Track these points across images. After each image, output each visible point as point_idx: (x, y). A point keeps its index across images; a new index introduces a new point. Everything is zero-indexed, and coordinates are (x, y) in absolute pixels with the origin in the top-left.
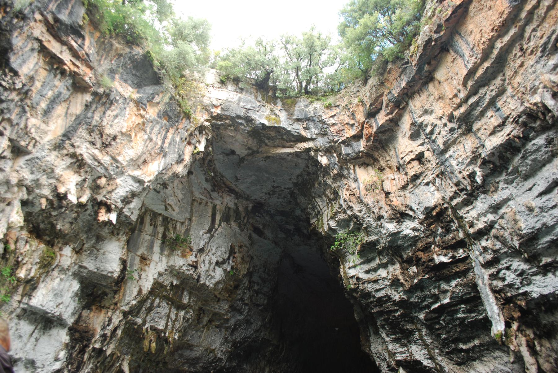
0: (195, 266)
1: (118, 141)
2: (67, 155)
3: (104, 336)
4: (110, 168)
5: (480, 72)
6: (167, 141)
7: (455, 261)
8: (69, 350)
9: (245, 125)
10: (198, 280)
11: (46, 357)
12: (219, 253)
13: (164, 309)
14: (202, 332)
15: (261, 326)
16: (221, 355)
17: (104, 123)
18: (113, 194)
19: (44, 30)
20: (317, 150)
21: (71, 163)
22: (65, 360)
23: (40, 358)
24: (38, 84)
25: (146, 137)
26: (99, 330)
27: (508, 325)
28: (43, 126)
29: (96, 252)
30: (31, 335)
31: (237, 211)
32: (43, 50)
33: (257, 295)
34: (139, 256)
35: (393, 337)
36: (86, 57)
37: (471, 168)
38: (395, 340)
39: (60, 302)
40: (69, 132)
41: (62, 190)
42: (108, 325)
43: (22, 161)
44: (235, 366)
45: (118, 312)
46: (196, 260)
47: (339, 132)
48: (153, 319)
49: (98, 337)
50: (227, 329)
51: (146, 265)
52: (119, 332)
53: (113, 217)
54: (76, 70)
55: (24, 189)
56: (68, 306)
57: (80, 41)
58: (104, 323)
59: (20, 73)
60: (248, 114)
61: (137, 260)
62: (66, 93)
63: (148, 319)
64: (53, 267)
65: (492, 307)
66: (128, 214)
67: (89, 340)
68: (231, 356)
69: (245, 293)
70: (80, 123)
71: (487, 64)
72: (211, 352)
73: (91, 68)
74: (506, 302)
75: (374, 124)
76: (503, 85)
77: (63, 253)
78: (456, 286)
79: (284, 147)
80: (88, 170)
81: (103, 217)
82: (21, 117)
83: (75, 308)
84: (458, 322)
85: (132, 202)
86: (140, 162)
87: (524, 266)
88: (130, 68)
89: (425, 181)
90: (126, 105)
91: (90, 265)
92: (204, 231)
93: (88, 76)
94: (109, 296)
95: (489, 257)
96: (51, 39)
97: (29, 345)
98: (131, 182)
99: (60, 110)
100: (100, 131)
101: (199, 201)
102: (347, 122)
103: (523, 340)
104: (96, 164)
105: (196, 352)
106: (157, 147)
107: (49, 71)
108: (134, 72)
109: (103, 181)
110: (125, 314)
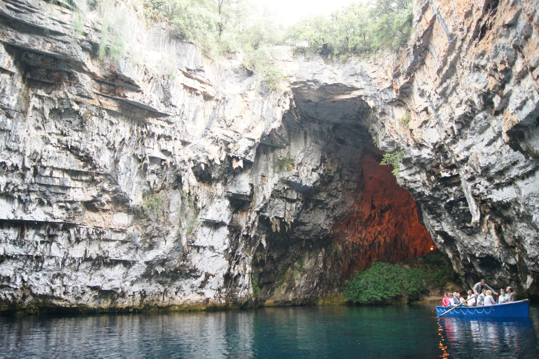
0: (297, 175)
3: (248, 228)
4: (234, 138)
5: (444, 72)
6: (264, 110)
7: (453, 177)
10: (301, 184)
12: (313, 163)
14: (311, 213)
15: (354, 204)
20: (366, 96)
24: (186, 106)
25: (251, 113)
26: (244, 224)
27: (482, 216)
30: (209, 234)
31: (322, 133)
32: (185, 87)
33: (348, 183)
35: (432, 216)
36: (208, 81)
37: (450, 123)
38: (433, 218)
41: (211, 158)
42: (249, 221)
43: (188, 147)
44: (338, 233)
47: (379, 84)
48: (276, 212)
49: (244, 228)
50: (328, 209)
52: (256, 224)
53: (241, 164)
54: (204, 90)
59: (177, 105)
61: (260, 178)
65: (473, 207)
67: (240, 231)
68: (334, 227)
71: (446, 68)
73: (212, 86)
74: (482, 202)
75: (398, 83)
76: (457, 81)
78: (456, 190)
79: (343, 94)
84: (461, 211)
87: (487, 184)
89: (431, 126)
91: (233, 190)
93: (210, 91)
95: (469, 176)
97: (209, 239)
102: (383, 77)
103: (493, 225)
104: (226, 137)
110: (258, 212)
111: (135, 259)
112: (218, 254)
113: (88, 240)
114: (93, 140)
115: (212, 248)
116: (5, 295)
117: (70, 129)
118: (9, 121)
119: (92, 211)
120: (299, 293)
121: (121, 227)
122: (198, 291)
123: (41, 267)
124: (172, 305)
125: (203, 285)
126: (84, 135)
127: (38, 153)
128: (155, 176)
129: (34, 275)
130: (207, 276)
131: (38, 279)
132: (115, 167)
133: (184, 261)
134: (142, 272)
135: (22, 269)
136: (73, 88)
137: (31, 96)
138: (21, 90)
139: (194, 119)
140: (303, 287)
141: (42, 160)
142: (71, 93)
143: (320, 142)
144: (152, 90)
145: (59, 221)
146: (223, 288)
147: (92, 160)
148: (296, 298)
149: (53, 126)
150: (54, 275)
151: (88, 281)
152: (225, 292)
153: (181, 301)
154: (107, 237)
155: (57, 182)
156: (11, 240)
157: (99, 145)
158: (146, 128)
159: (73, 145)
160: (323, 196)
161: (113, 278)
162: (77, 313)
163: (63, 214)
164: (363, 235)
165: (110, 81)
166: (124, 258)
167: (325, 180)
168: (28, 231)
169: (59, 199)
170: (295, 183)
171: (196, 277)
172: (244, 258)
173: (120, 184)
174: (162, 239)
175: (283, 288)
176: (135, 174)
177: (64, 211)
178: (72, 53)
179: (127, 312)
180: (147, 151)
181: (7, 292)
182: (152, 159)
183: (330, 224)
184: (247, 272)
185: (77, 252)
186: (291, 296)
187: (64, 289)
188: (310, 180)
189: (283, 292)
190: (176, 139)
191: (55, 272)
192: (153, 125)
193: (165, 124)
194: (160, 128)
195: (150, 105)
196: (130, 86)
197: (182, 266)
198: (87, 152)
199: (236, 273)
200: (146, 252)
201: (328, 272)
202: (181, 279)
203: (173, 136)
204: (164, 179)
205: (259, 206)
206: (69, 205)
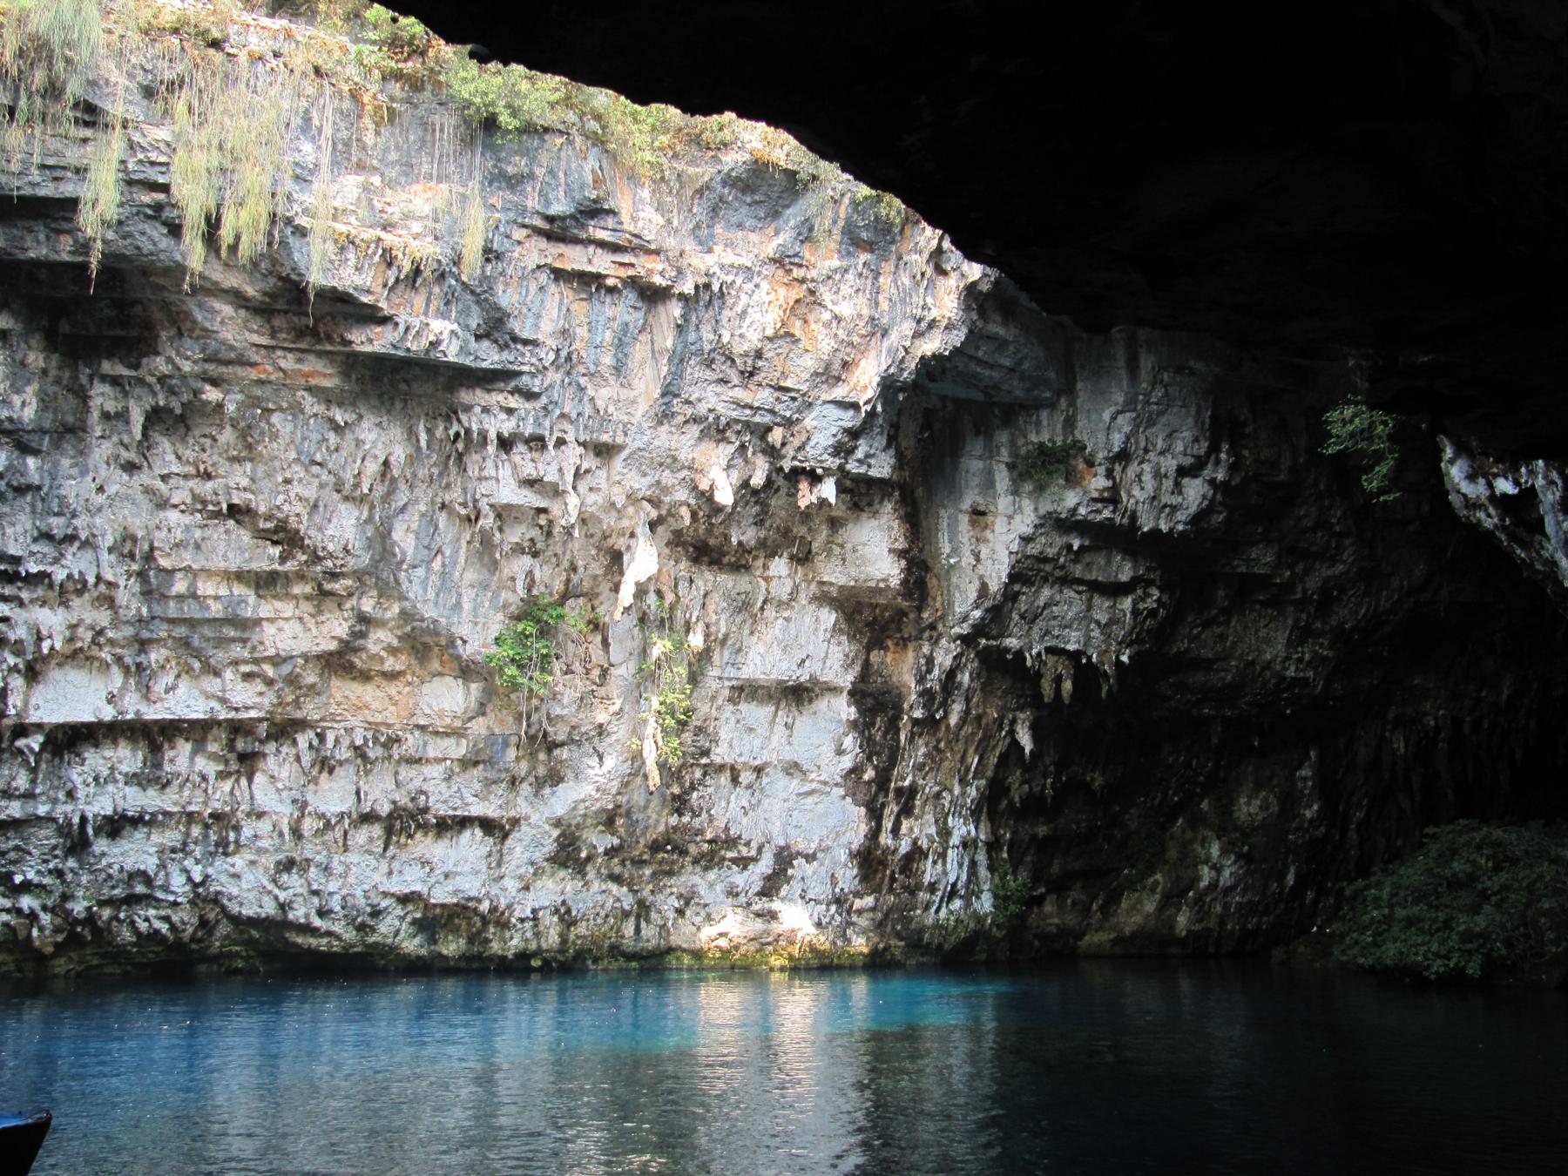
0: (1112, 498)
2: (686, 422)
3: (927, 695)
12: (1180, 447)
13: (1070, 603)
14: (1228, 623)
16: (1297, 670)
18: (808, 448)
19: (543, 243)
24: (582, 332)
28: (625, 394)
29: (837, 550)
30: (773, 721)
32: (559, 275)
34: (966, 512)
36: (636, 241)
41: (704, 485)
42: (929, 671)
43: (618, 462)
45: (943, 641)
46: (1109, 484)
48: (1047, 632)
49: (914, 697)
50: (1301, 604)
51: (986, 527)
53: (828, 490)
54: (631, 272)
57: (610, 222)
58: (919, 669)
59: (540, 337)
61: (964, 520)
64: (759, 605)
66: (862, 470)
70: (682, 361)
73: (657, 252)
77: (770, 573)
80: (739, 427)
81: (806, 497)
82: (581, 401)
83: (847, 656)
85: (856, 447)
91: (835, 575)
92: (1113, 409)
93: (656, 272)
96: (562, 248)
97: (775, 739)
99: (639, 351)
104: (748, 412)
107: (589, 299)
108: (749, 200)
110: (967, 640)
111: (512, 813)
112: (821, 787)
113: (359, 761)
114: (287, 481)
116: (147, 919)
117: (215, 458)
118: (31, 462)
119: (354, 679)
120: (1219, 909)
121: (448, 721)
122: (755, 907)
123: (237, 842)
124: (670, 950)
125: (770, 887)
126: (261, 469)
127: (134, 539)
128: (527, 560)
129: (220, 863)
131: (236, 876)
132: (384, 550)
133: (680, 815)
134: (545, 850)
135: (182, 850)
136: (188, 342)
137: (84, 380)
138: (45, 372)
139: (618, 369)
141: (157, 553)
142: (187, 358)
143: (1199, 366)
144: (432, 307)
145: (253, 714)
146: (858, 895)
147: (302, 539)
148: (1207, 930)
149: (167, 455)
150: (278, 863)
151: (385, 879)
152: (873, 909)
154: (412, 751)
155: (216, 610)
156: (126, 775)
157: (310, 493)
158: (459, 421)
159: (236, 501)
160: (1262, 558)
161: (456, 870)
162: (360, 968)
163: (261, 694)
164: (1506, 692)
165: (289, 302)
166: (477, 809)
167: (1244, 508)
168: (172, 748)
169: (234, 655)
171: (743, 863)
172: (938, 796)
173: (411, 595)
174: (587, 747)
175: (1153, 890)
176: (462, 560)
177: (261, 687)
178: (138, 248)
179: (518, 968)
180: (483, 488)
181: (152, 912)
182: (504, 514)
184: (955, 840)
185: (333, 796)
187: (316, 900)
188: (1174, 509)
189: (1150, 907)
190: (561, 442)
191: (281, 856)
192: (478, 410)
193: (514, 402)
194: (503, 416)
195: (432, 355)
196: (350, 309)
197: (676, 829)
198: (279, 515)
199: (905, 846)
200: (547, 791)
201: (1352, 835)
203: (547, 434)
204: (566, 564)
205: (965, 619)
206: (269, 670)
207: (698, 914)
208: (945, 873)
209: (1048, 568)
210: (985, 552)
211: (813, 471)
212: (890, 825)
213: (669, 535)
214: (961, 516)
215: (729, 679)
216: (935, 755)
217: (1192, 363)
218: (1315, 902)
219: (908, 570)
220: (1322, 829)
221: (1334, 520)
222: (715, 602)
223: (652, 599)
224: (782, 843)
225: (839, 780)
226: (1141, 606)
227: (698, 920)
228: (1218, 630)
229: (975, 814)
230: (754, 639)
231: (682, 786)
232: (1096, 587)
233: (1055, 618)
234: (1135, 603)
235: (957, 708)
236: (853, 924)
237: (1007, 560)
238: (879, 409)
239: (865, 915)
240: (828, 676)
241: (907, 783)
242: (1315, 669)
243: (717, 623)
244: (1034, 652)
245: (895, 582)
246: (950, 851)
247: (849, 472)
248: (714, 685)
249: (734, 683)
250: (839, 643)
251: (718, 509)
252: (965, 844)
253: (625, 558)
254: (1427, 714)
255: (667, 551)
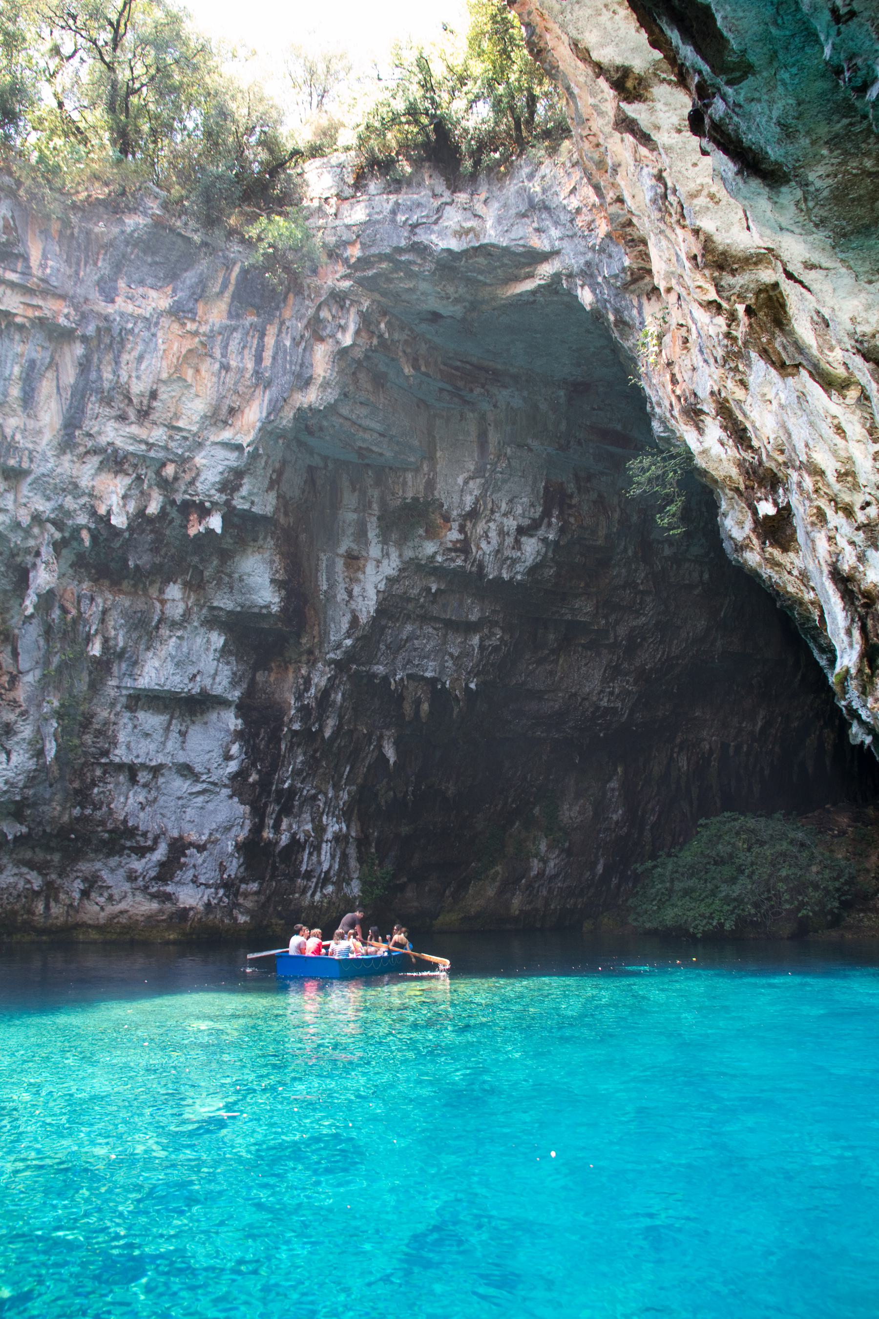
0: (463, 548)
1: (163, 396)
2: (87, 453)
3: (305, 711)
4: (172, 444)
6: (268, 355)
8: (247, 742)
9: (419, 261)
11: (207, 757)
12: (519, 510)
13: (428, 638)
16: (609, 701)
17: (124, 379)
18: (198, 484)
20: (570, 276)
21: (101, 462)
22: (243, 756)
23: (198, 760)
25: (217, 366)
28: (31, 424)
29: (226, 579)
30: (167, 729)
36: (42, 285)
39: (195, 672)
40: (73, 417)
41: (102, 510)
42: (307, 690)
43: (25, 488)
45: (320, 665)
46: (462, 537)
48: (409, 662)
49: (293, 712)
51: (359, 569)
53: (215, 522)
55: (49, 526)
56: (216, 674)
58: (298, 688)
60: (416, 239)
61: (340, 564)
62: (41, 356)
63: (399, 663)
66: (246, 506)
69: (636, 571)
72: (584, 699)
79: (517, 279)
83: (234, 674)
85: (241, 485)
86: (222, 415)
88: (137, 256)
90: (153, 330)
91: (225, 602)
92: (466, 475)
93: (61, 313)
94: (292, 641)
97: (170, 745)
98: (221, 453)
99: (46, 387)
100: (122, 393)
101: (444, 414)
105: (552, 703)
106: (248, 376)
108: (149, 260)
109: (170, 470)
110: (340, 666)
112: (212, 787)
115: (186, 771)
120: (545, 893)
125: (167, 870)
130: (179, 847)
133: (83, 808)
140: (556, 876)
143: (535, 444)
146: (243, 880)
152: (257, 893)
153: (102, 914)
164: (760, 724)
170: (459, 573)
171: (142, 852)
172: (314, 798)
175: (494, 879)
183: (629, 693)
184: (329, 835)
186: (517, 903)
188: (514, 561)
189: (491, 892)
197: (78, 819)
199: (285, 839)
201: (647, 834)
202: (92, 855)
205: (339, 646)
207: (101, 895)
208: (320, 863)
209: (410, 606)
210: (356, 590)
211: (202, 503)
212: (272, 822)
213: (72, 557)
214: (337, 559)
215: (127, 688)
216: (312, 764)
217: (530, 441)
218: (618, 887)
219: (286, 600)
220: (625, 829)
221: (639, 581)
222: (115, 619)
223: (56, 613)
224: (176, 834)
225: (227, 782)
226: (487, 643)
227: (101, 900)
228: (549, 668)
229: (346, 815)
230: (150, 654)
231: (83, 781)
232: (450, 625)
233: (415, 650)
234: (482, 640)
235: (331, 724)
236: (240, 905)
237: (375, 598)
238: (261, 451)
239: (250, 898)
240: (218, 690)
241: (286, 786)
242: (623, 700)
243: (116, 638)
244: (398, 677)
245: (275, 609)
246: (324, 845)
247: (235, 508)
248: (113, 693)
249: (132, 692)
250: (228, 663)
251: (115, 532)
252: (338, 838)
253: (31, 575)
254: (704, 740)
255: (71, 571)
